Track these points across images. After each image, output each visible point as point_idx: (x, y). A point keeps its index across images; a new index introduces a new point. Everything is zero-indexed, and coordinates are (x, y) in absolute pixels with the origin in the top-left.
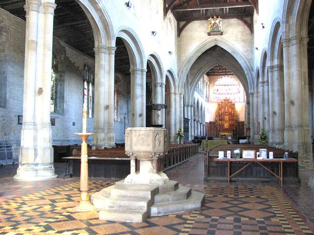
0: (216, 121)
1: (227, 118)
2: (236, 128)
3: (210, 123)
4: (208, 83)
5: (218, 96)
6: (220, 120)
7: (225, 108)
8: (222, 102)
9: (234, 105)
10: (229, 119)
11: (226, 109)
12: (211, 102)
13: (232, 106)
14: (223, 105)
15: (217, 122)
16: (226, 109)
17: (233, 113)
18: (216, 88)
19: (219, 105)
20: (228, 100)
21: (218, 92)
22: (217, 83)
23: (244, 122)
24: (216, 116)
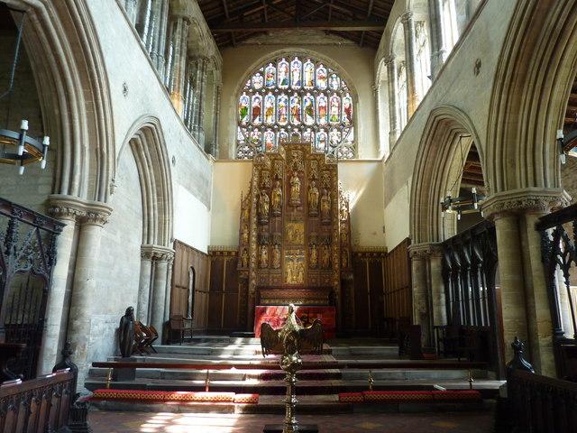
0: (244, 245)
1: (296, 230)
2: (343, 282)
3: (214, 255)
4: (217, 74)
5: (255, 135)
6: (260, 243)
7: (290, 186)
8: (275, 158)
9: (332, 170)
10: (308, 238)
11: (296, 188)
12: (223, 157)
13: (324, 174)
14: (280, 168)
15: (247, 250)
16: (296, 188)
17: (326, 207)
18: (244, 100)
19: (259, 167)
20: (304, 148)
21: (257, 122)
22: (257, 81)
23: (379, 256)
24: (245, 223)
